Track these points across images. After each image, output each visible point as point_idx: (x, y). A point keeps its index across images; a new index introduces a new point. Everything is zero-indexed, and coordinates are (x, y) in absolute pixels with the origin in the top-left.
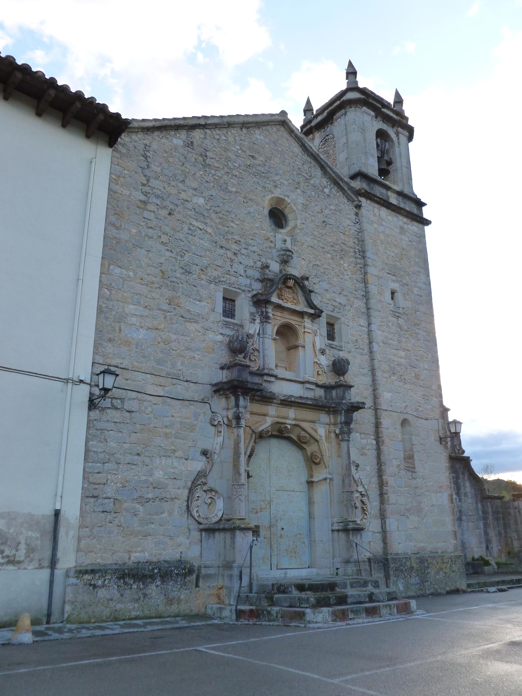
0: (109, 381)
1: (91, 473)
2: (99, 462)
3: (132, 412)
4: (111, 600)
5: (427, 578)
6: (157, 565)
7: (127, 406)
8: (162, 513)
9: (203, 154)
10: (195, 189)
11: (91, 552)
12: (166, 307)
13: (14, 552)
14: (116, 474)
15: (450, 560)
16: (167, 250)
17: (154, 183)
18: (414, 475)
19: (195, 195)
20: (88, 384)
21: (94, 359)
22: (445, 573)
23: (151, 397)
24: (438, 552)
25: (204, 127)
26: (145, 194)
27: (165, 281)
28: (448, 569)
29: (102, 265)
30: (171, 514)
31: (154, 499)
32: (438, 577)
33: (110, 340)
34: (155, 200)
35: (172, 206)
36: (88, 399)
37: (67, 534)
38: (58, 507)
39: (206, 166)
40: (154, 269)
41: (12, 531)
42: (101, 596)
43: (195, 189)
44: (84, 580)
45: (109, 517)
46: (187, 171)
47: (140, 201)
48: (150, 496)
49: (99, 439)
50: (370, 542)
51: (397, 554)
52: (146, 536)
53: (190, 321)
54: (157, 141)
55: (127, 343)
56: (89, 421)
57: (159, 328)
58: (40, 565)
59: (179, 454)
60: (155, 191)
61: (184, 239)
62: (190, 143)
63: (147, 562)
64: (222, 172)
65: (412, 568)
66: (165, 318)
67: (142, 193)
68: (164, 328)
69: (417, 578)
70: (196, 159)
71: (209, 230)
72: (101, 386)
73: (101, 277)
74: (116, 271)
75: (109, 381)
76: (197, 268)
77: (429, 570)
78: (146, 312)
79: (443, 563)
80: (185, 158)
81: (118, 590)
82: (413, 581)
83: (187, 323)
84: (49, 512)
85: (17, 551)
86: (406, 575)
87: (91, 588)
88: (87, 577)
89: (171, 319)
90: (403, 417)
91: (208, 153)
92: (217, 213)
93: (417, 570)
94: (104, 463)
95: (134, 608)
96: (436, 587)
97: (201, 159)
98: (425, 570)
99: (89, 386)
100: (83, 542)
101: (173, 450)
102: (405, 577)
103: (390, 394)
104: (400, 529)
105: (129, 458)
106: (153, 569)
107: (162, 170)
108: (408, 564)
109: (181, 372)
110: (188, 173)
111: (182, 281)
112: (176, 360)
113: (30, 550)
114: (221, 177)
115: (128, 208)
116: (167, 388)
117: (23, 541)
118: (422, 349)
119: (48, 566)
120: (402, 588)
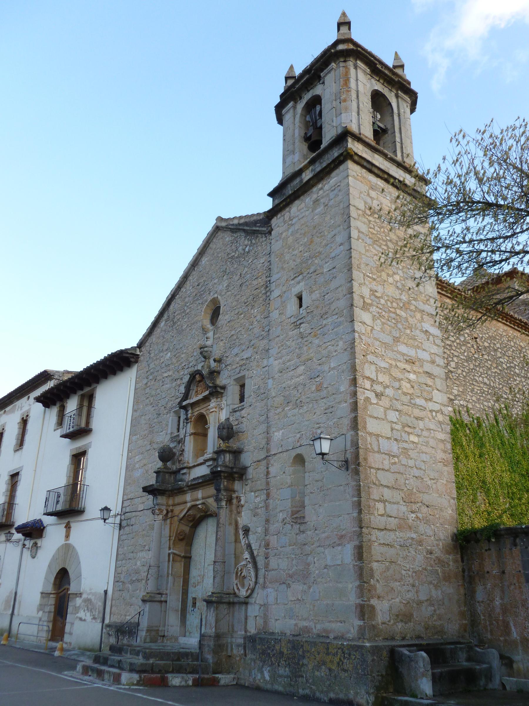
5: (301, 671)
15: (340, 651)
18: (302, 528)
22: (330, 670)
24: (328, 637)
28: (336, 665)
32: (317, 673)
50: (256, 617)
51: (273, 633)
65: (281, 653)
69: (287, 669)
77: (305, 661)
79: (328, 654)
82: (281, 671)
86: (274, 662)
90: (294, 453)
93: (289, 658)
96: (314, 687)
98: (299, 660)
102: (272, 664)
103: (281, 432)
104: (278, 602)
108: (277, 647)
118: (329, 344)
120: (267, 678)
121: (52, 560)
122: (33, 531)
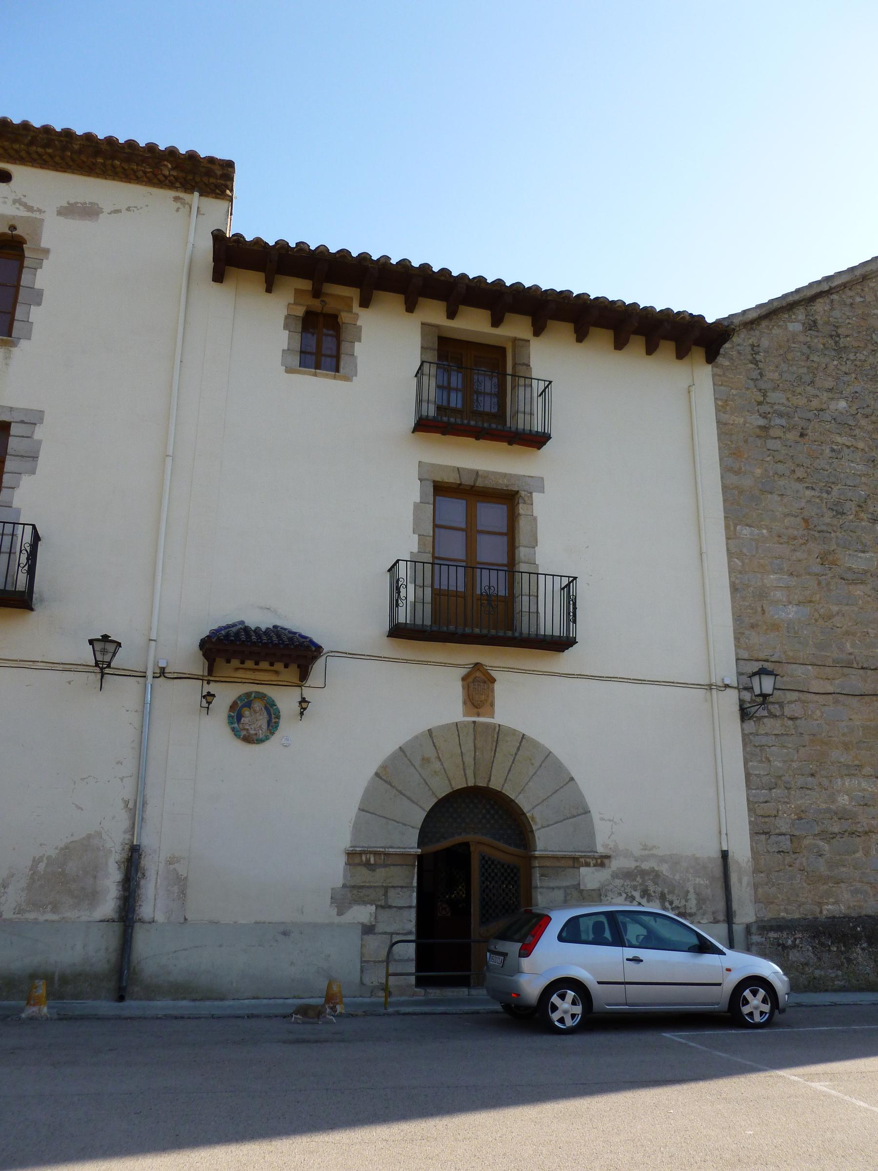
0: (767, 684)
1: (756, 803)
2: (763, 788)
3: (796, 718)
4: (807, 964)
6: (861, 920)
7: (787, 711)
8: (854, 853)
9: (834, 333)
10: (830, 390)
11: (772, 903)
12: (817, 569)
13: (683, 902)
14: (788, 803)
16: (807, 488)
17: (773, 397)
19: (832, 399)
20: (735, 688)
21: (737, 654)
23: (818, 696)
25: (829, 292)
26: (764, 416)
27: (812, 532)
29: (727, 527)
30: (867, 853)
31: (842, 834)
33: (753, 626)
34: (778, 421)
35: (803, 423)
36: (738, 708)
37: (740, 881)
38: (725, 848)
39: (840, 350)
40: (793, 518)
41: (677, 877)
42: (794, 959)
43: (830, 390)
44: (769, 938)
45: (788, 859)
46: (815, 365)
47: (760, 427)
48: (836, 829)
49: (759, 758)
52: (838, 883)
53: (854, 582)
54: (769, 337)
55: (775, 627)
56: (744, 736)
57: (813, 599)
58: (715, 918)
59: (867, 770)
60: (776, 407)
61: (827, 467)
62: (811, 323)
63: (844, 918)
64: (865, 352)
66: (819, 583)
67: (760, 415)
68: (820, 599)
70: (824, 345)
71: (861, 445)
72: (757, 691)
73: (727, 544)
74: (745, 532)
75: (767, 684)
76: (853, 506)
78: (793, 582)
80: (809, 347)
81: (813, 953)
83: (851, 587)
84: (716, 855)
85: (687, 901)
87: (780, 948)
88: (772, 935)
89: (828, 584)
91: (840, 331)
92: (867, 417)
94: (770, 789)
95: (837, 976)
97: (831, 342)
99: (736, 691)
100: (760, 890)
101: (858, 766)
105: (800, 781)
106: (855, 927)
107: (781, 375)
109: (853, 657)
110: (817, 369)
111: (835, 528)
112: (843, 640)
113: (701, 900)
114: (865, 361)
115: (746, 441)
116: (837, 682)
117: (691, 890)
119: (724, 920)
121: (393, 758)
122: (255, 660)
